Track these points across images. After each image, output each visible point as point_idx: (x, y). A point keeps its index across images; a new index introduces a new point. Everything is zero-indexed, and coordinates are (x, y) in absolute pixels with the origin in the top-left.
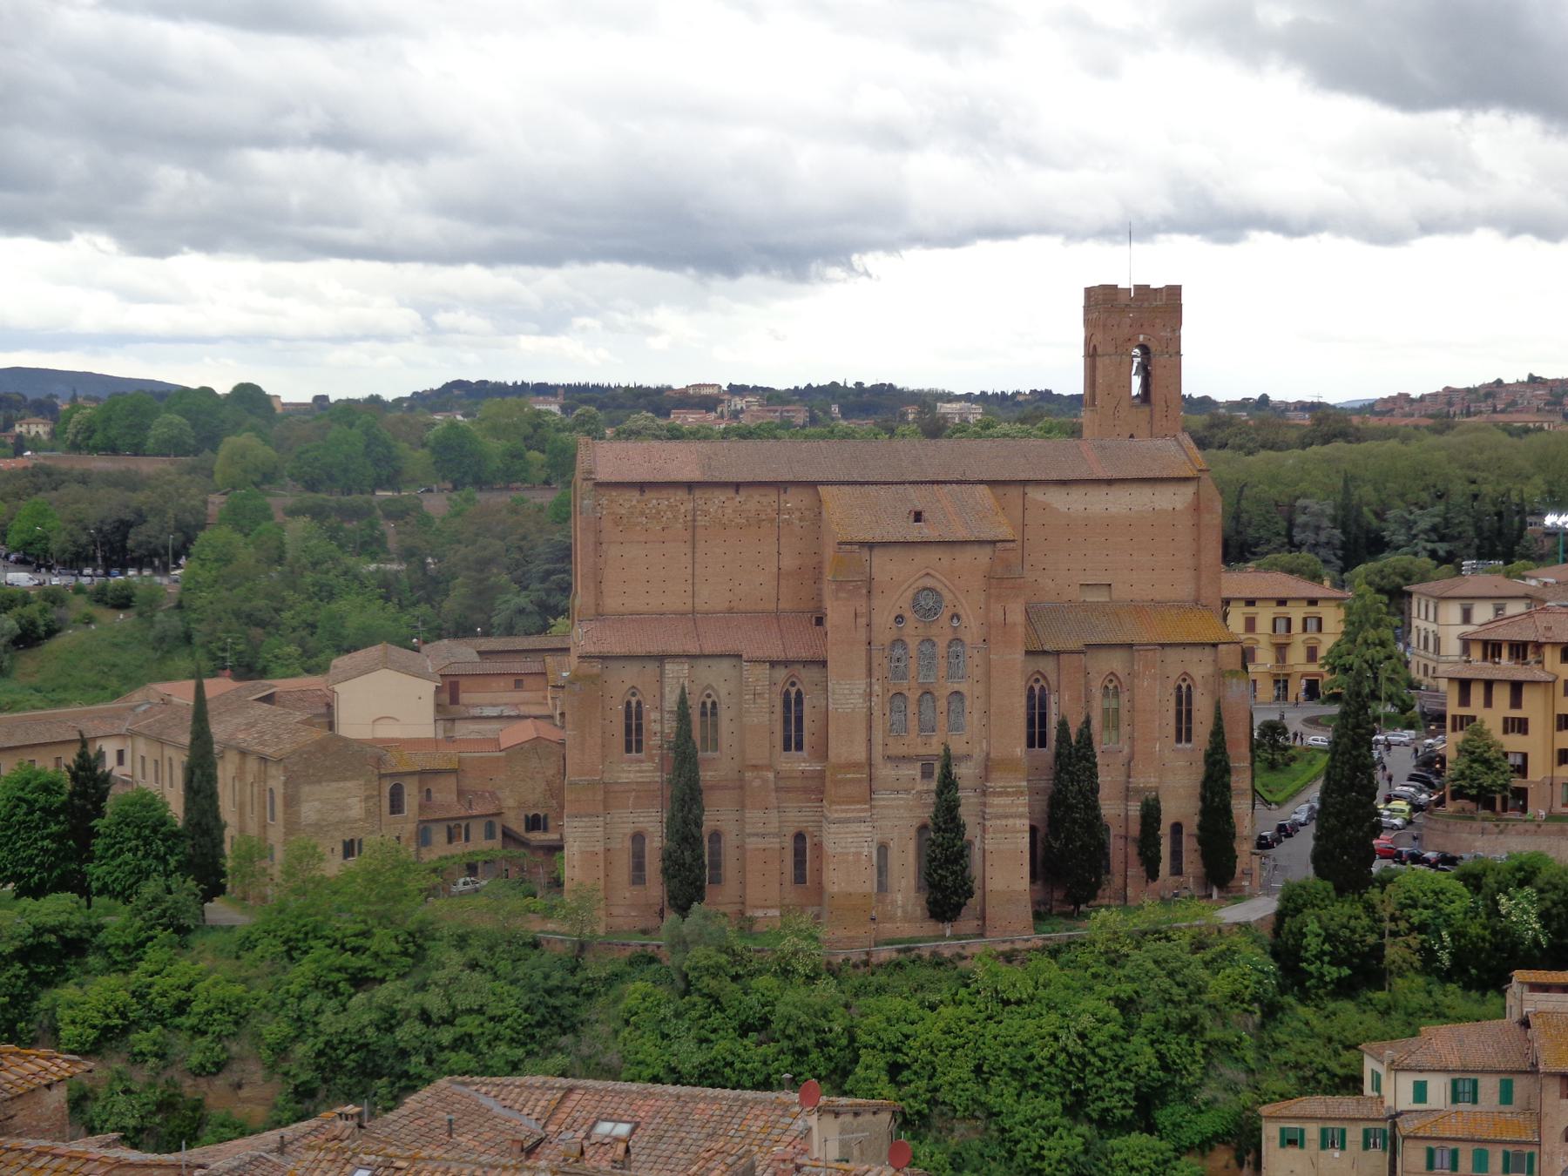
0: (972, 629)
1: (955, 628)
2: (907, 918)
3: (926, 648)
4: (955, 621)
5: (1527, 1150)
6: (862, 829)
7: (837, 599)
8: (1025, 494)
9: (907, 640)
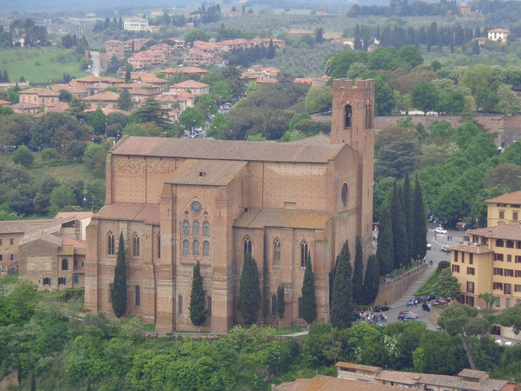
2: (188, 324)
8: (264, 166)
9: (189, 220)
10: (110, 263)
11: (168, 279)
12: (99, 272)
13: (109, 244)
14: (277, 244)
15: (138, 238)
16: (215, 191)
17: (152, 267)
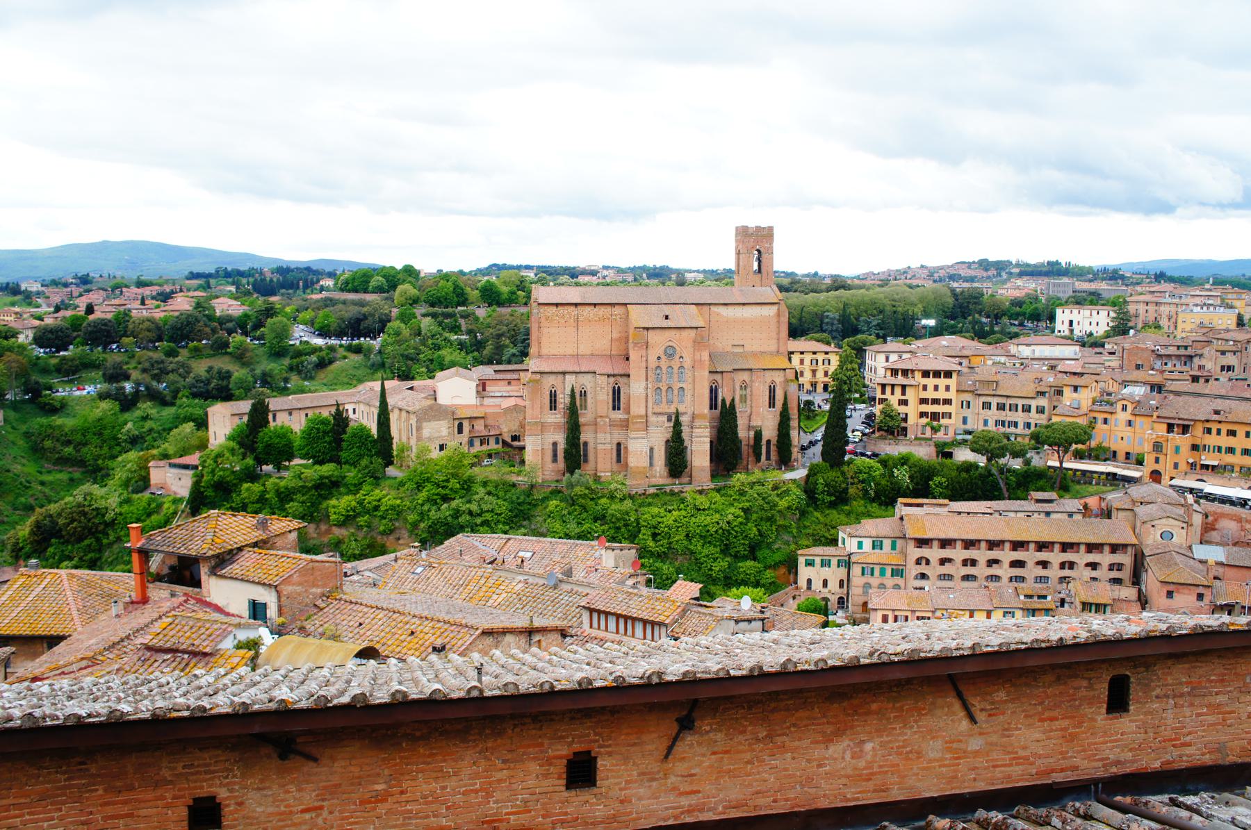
0: (687, 362)
2: (660, 477)
3: (669, 370)
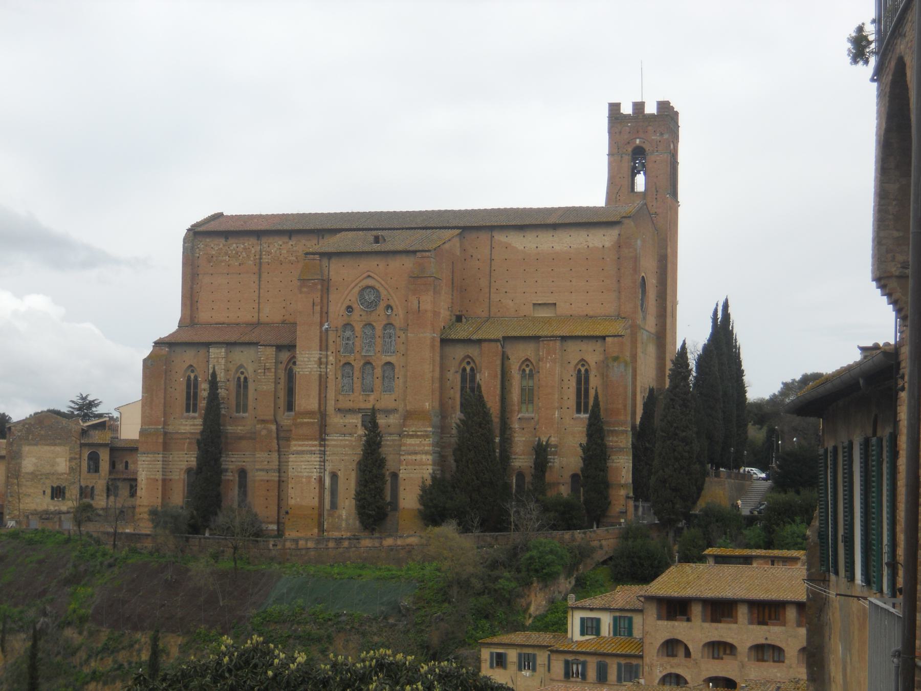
0: (398, 322)
1: (388, 316)
3: (368, 331)
4: (390, 311)
5: (634, 662)
6: (313, 459)
7: (301, 292)
9: (354, 324)
10: (188, 428)
11: (311, 440)
12: (166, 447)
13: (188, 393)
14: (530, 370)
15: (246, 378)
16: (408, 263)
17: (274, 427)
